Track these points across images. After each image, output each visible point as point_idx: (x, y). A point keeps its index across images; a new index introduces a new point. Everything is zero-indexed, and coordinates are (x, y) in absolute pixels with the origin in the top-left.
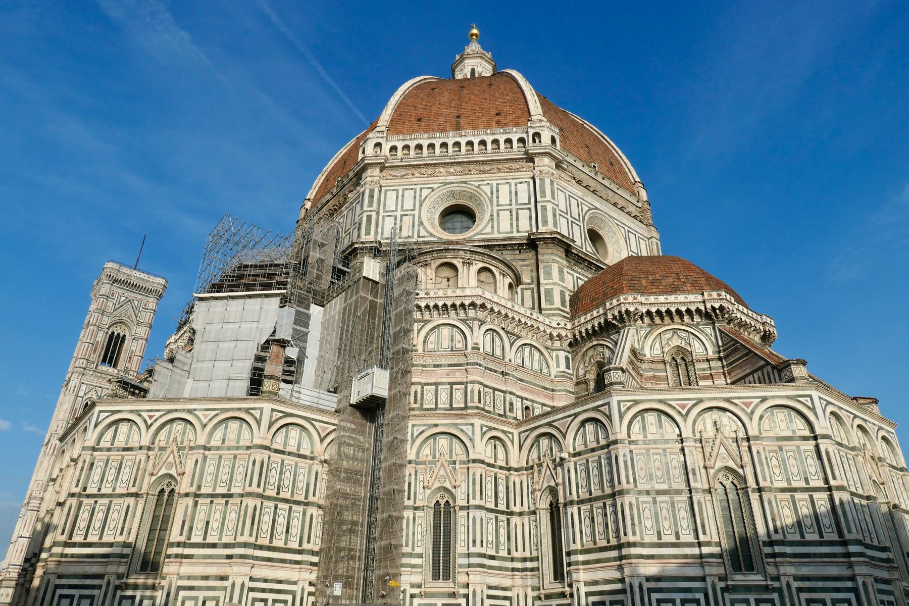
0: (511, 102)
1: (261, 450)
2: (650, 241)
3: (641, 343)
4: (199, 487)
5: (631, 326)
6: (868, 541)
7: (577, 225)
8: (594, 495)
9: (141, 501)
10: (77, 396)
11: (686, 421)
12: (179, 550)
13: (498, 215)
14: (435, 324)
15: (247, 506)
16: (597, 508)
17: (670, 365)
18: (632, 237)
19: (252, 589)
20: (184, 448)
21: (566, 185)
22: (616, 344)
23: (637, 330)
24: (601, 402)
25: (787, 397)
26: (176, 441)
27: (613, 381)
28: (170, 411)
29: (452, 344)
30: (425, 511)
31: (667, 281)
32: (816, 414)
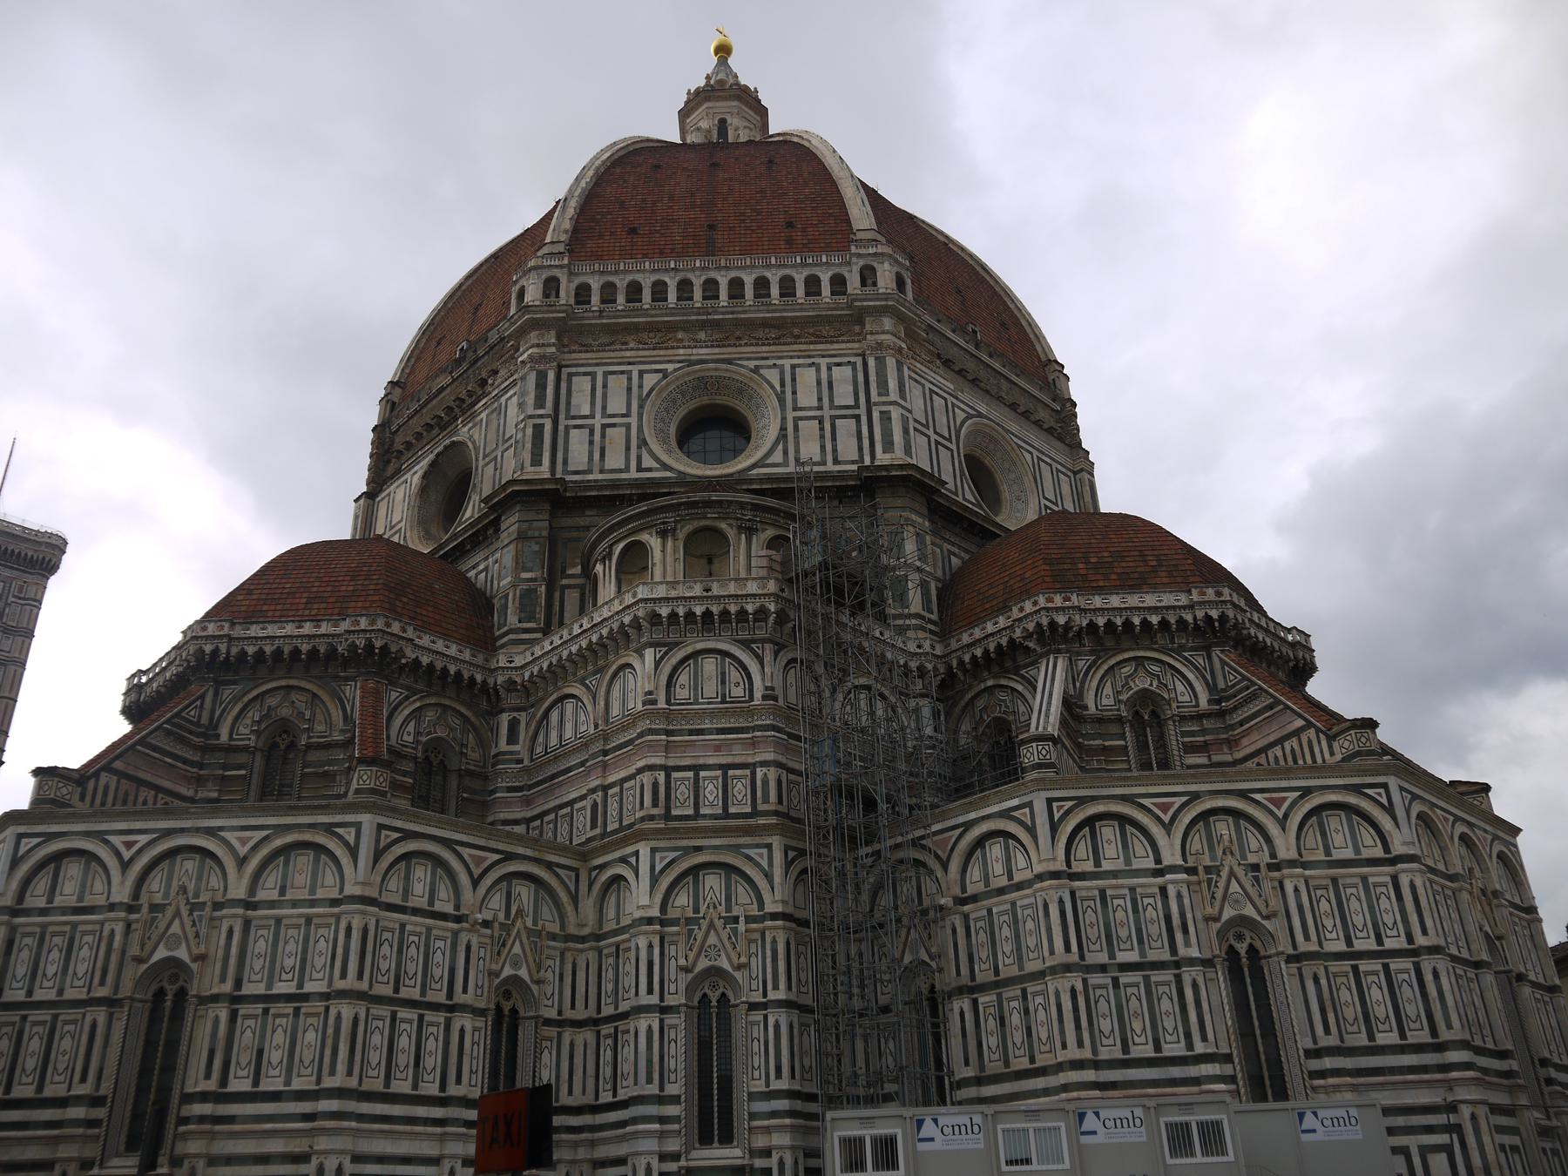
2: (1078, 476)
3: (1078, 685)
4: (238, 984)
5: (1059, 651)
6: (1478, 1042)
9: (122, 1015)
12: (206, 1109)
14: (689, 650)
15: (339, 1017)
17: (1132, 726)
18: (1045, 468)
21: (924, 369)
23: (1070, 660)
24: (1015, 802)
25: (1345, 787)
26: (185, 892)
27: (1037, 761)
28: (168, 833)
29: (723, 689)
30: (683, 1015)
31: (1124, 564)
32: (1394, 818)
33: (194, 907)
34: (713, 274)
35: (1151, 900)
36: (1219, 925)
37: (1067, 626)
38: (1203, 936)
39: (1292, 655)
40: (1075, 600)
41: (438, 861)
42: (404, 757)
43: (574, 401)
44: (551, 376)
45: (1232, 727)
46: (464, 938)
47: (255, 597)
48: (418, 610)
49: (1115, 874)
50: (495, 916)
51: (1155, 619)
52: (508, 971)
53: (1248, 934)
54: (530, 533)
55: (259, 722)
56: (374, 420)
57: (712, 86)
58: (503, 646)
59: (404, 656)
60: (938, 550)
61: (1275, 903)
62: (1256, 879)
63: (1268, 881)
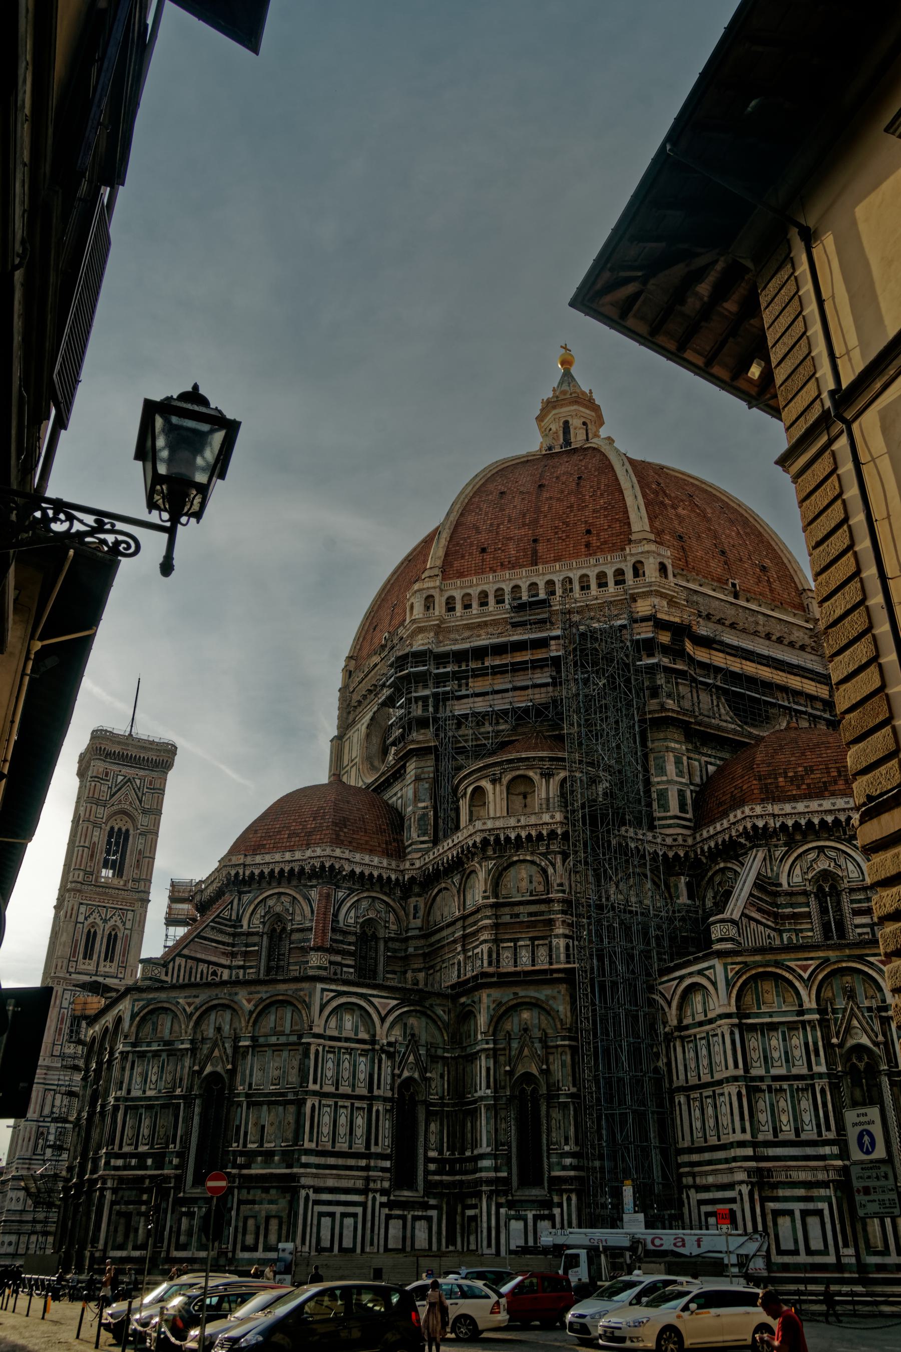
0: (606, 509)
5: (760, 846)
10: (77, 922)
16: (707, 1097)
17: (816, 896)
19: (317, 1202)
23: (769, 851)
31: (812, 776)
34: (535, 579)
40: (769, 808)
42: (349, 933)
47: (259, 835)
48: (354, 836)
51: (830, 819)
52: (406, 1074)
54: (422, 776)
55: (264, 917)
56: (339, 685)
57: (557, 397)
58: (409, 853)
59: (344, 870)
60: (697, 763)
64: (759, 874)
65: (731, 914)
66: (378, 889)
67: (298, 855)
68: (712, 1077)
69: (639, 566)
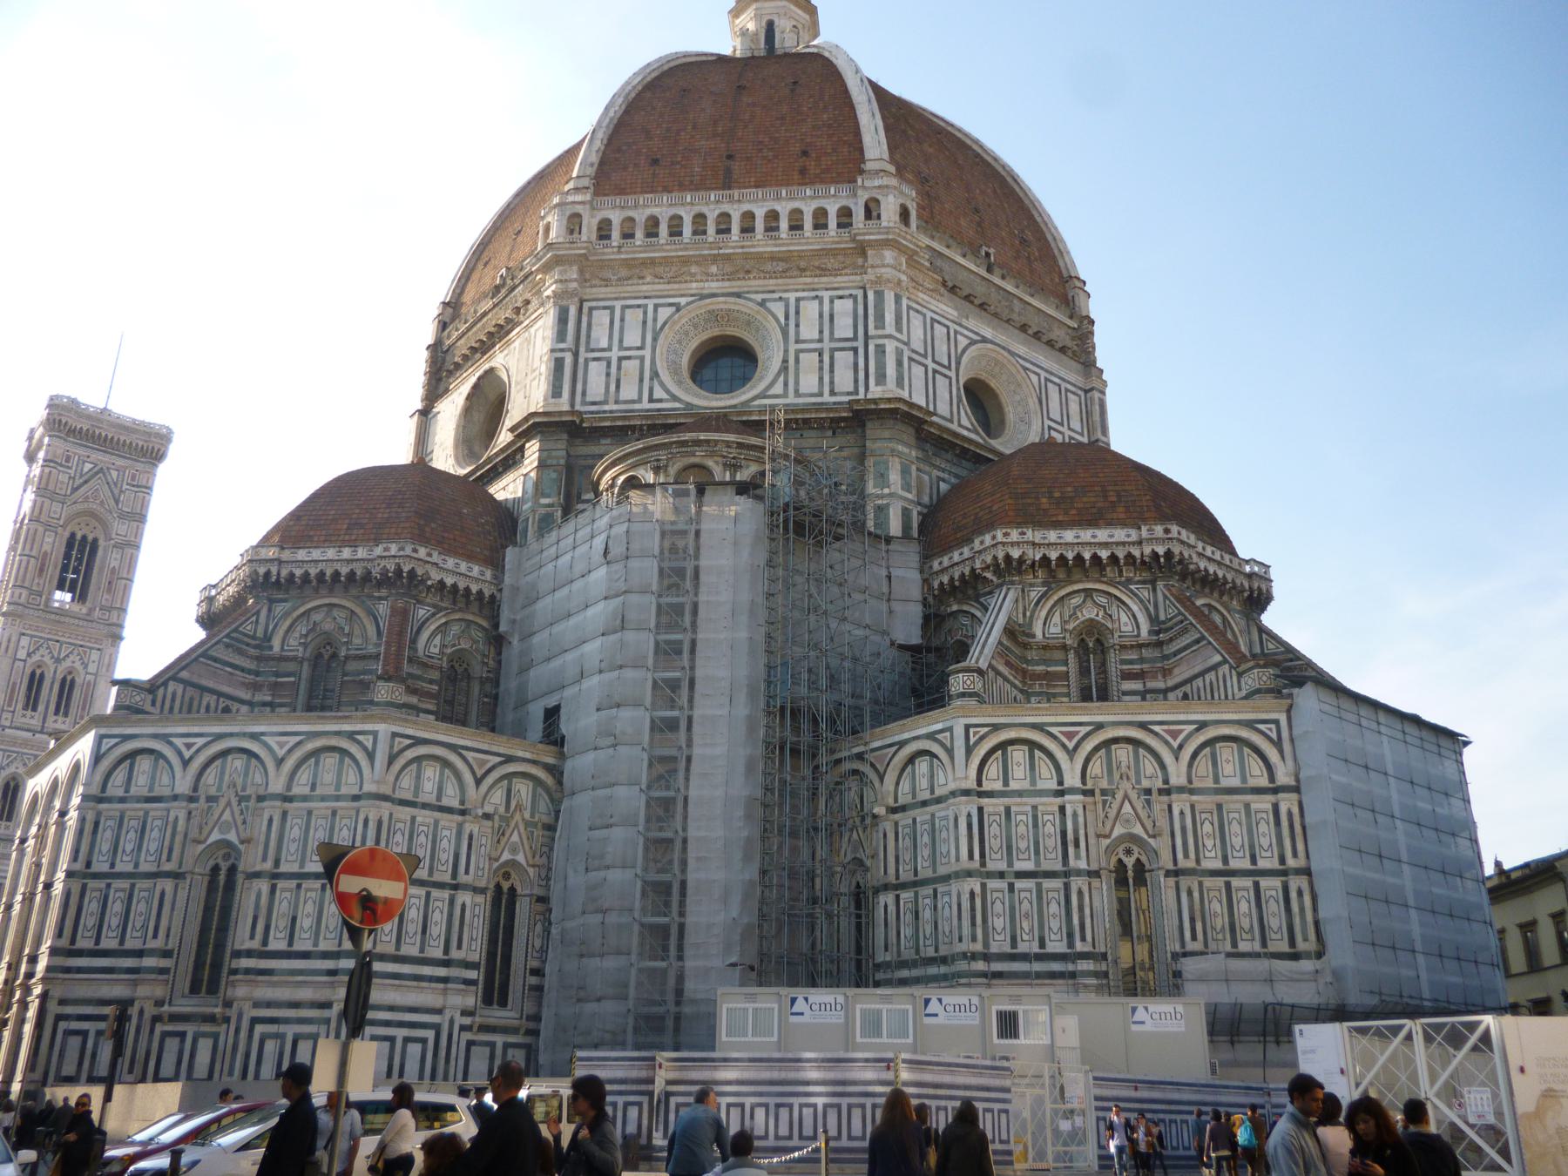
0: (830, 126)
1: (377, 802)
2: (1089, 395)
3: (1028, 614)
4: (277, 863)
5: (1013, 583)
7: (945, 376)
8: (920, 876)
10: (15, 659)
11: (1071, 760)
13: (797, 360)
20: (248, 798)
21: (925, 297)
22: (987, 610)
23: (1023, 591)
24: (939, 726)
26: (235, 786)
31: (1085, 499)
33: (241, 799)
34: (726, 208)
35: (1051, 817)
36: (1108, 841)
37: (1021, 560)
38: (1093, 850)
39: (1247, 587)
40: (1030, 535)
41: (446, 763)
42: (432, 667)
43: (594, 334)
44: (573, 311)
45: (1165, 657)
46: (468, 828)
49: (1020, 794)
50: (496, 809)
52: (506, 856)
53: (1136, 849)
54: (549, 462)
55: (306, 636)
59: (430, 578)
61: (1163, 823)
62: (1148, 802)
63: (1160, 803)
64: (1009, 618)
65: (977, 662)
66: (476, 611)
67: (362, 553)
68: (935, 871)
69: (872, 205)
